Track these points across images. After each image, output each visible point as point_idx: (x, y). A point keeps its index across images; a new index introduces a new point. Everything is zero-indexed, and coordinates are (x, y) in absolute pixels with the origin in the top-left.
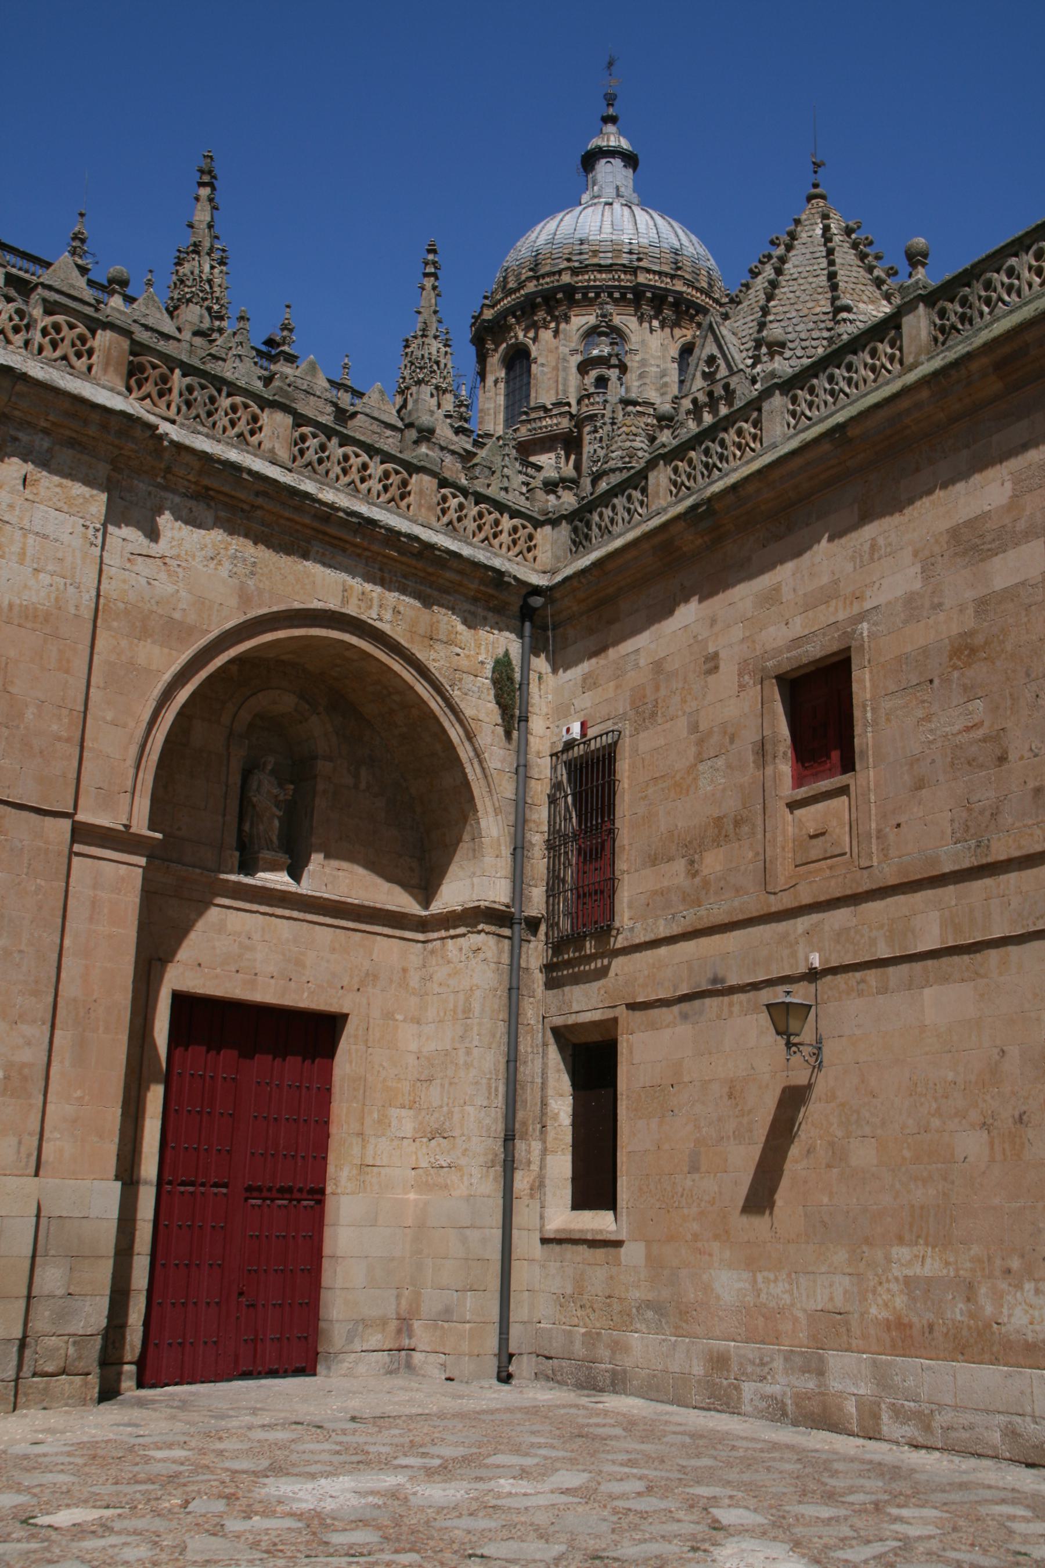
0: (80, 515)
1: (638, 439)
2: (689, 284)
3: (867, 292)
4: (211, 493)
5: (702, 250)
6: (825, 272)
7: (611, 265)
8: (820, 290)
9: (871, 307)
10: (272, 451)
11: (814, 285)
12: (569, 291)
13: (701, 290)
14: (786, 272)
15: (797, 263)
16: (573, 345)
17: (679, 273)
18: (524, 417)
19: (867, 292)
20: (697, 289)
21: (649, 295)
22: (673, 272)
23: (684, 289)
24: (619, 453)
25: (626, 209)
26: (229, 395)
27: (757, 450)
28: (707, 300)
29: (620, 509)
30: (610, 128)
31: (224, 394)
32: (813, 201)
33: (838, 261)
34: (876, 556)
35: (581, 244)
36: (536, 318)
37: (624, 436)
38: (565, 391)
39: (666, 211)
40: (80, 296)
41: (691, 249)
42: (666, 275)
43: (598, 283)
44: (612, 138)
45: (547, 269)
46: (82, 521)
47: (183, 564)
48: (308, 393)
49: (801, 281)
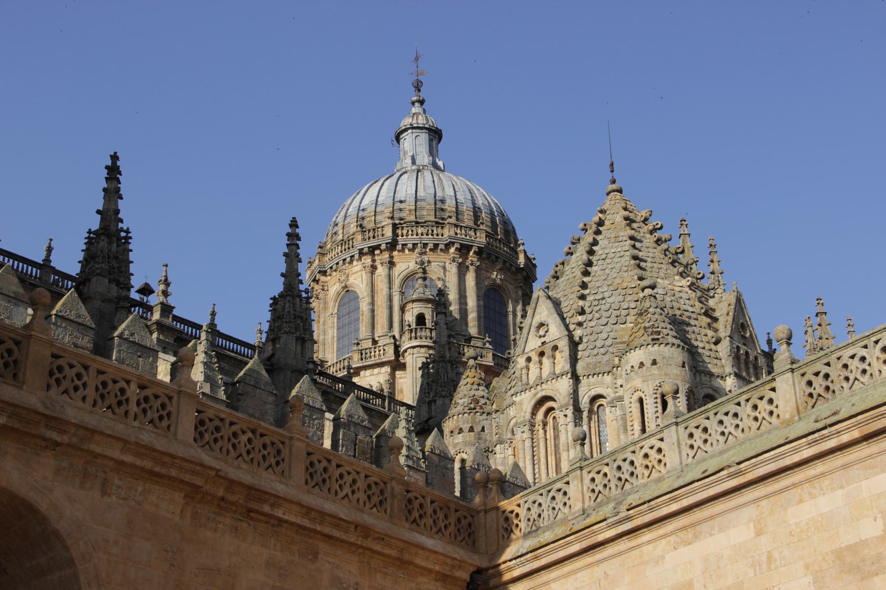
1: (481, 388)
4: (252, 514)
6: (628, 253)
7: (425, 222)
15: (604, 246)
21: (457, 246)
24: (466, 400)
29: (544, 506)
32: (612, 194)
34: (773, 566)
44: (420, 117)
48: (255, 387)
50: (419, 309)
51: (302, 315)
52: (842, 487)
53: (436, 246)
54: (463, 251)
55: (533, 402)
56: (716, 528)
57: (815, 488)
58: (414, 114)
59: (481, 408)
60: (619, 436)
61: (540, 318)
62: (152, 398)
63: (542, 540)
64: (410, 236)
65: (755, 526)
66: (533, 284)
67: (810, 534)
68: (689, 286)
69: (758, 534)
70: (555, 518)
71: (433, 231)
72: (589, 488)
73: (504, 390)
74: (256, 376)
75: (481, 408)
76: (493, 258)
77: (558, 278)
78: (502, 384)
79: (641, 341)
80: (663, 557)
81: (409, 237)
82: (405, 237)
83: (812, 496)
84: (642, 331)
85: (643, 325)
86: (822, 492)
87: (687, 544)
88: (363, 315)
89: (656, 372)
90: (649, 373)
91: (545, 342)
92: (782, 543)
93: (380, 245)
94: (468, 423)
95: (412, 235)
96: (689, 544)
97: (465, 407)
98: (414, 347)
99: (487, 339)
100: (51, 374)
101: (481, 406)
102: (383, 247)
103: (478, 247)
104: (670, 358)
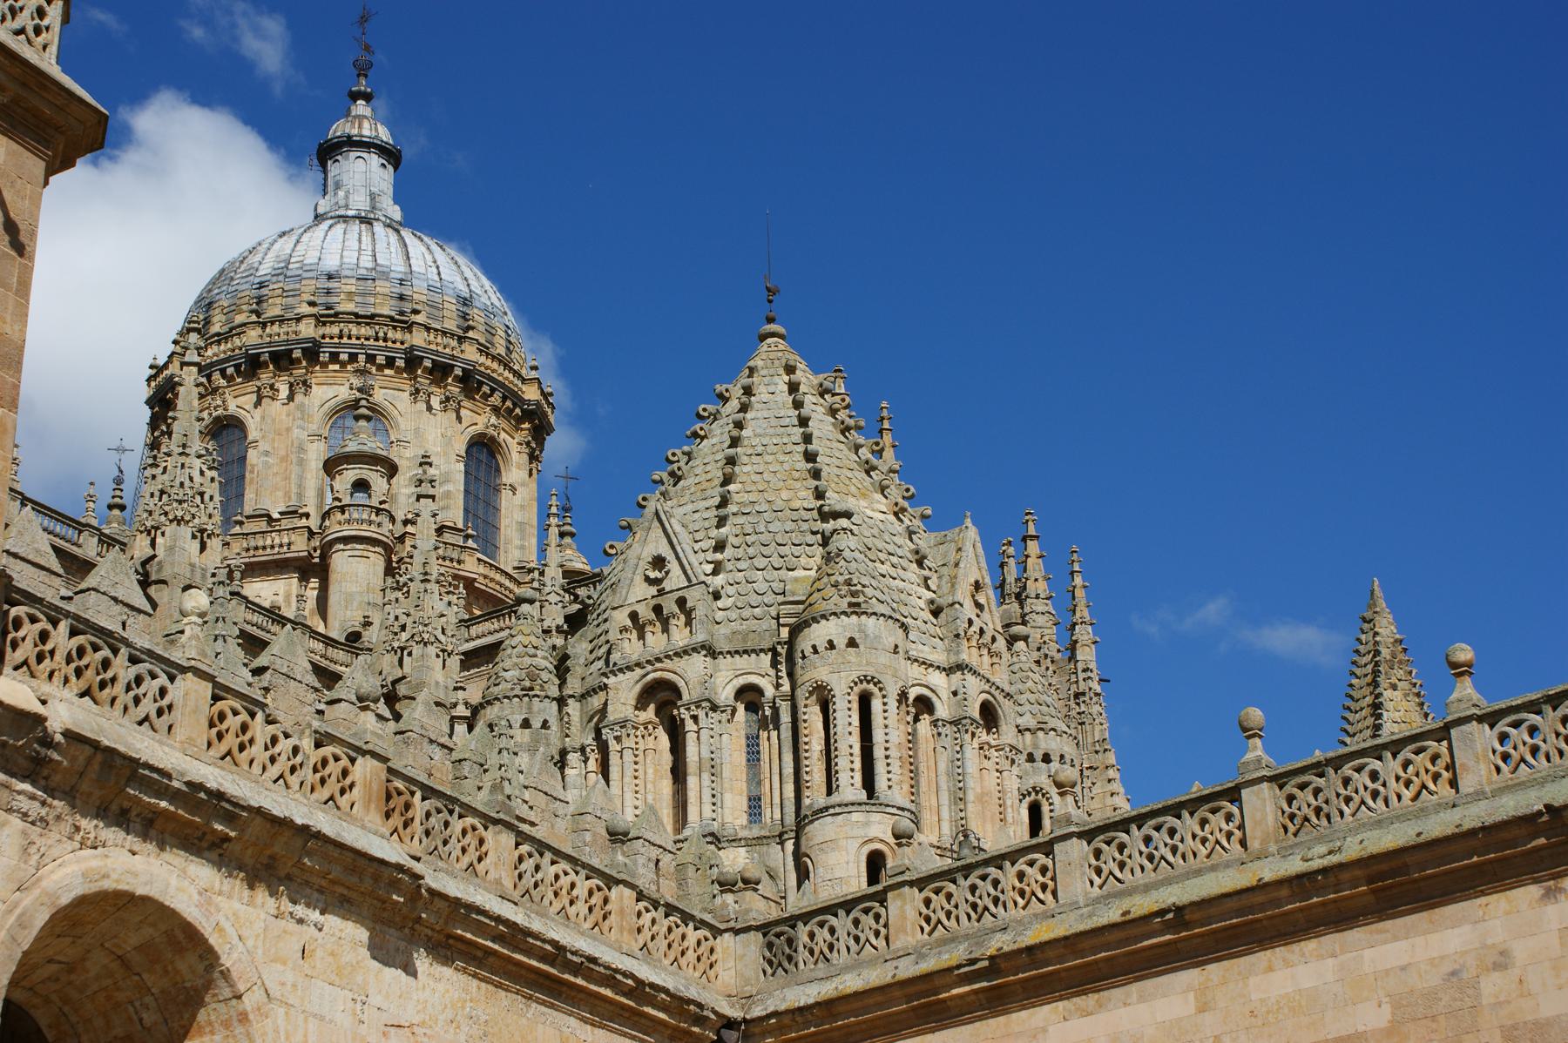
0: (349, 987)
2: (484, 350)
3: (854, 480)
6: (801, 448)
7: (373, 316)
8: (797, 475)
9: (863, 503)
10: (498, 882)
11: (786, 466)
13: (495, 358)
14: (746, 443)
15: (759, 431)
16: (313, 428)
18: (237, 529)
19: (854, 480)
20: (494, 358)
21: (428, 363)
22: (460, 333)
25: (390, 231)
26: (461, 817)
27: (1047, 902)
28: (506, 373)
30: (361, 107)
31: (456, 815)
32: (770, 340)
33: (816, 433)
37: (520, 649)
38: (300, 495)
40: (47, 566)
41: (484, 299)
43: (354, 341)
44: (366, 124)
45: (277, 311)
46: (350, 995)
47: (428, 1032)
48: (288, 677)
49: (769, 458)
50: (358, 471)
51: (204, 489)
52: (1334, 956)
53: (390, 362)
54: (435, 373)
55: (638, 688)
56: (1135, 995)
57: (1293, 952)
58: (355, 117)
59: (542, 689)
61: (657, 548)
62: (331, 760)
63: (840, 987)
64: (345, 339)
65: (1196, 998)
66: (547, 437)
67: (1281, 1017)
68: (896, 514)
69: (1202, 1009)
70: (858, 954)
71: (386, 334)
72: (920, 914)
73: (582, 661)
74: (289, 658)
75: (542, 689)
77: (679, 479)
78: (579, 651)
79: (829, 606)
80: (1044, 1030)
81: (342, 341)
82: (336, 340)
83: (1288, 964)
84: (830, 591)
86: (1303, 960)
87: (1084, 1014)
88: (252, 472)
89: (853, 660)
90: (840, 660)
91: (664, 589)
92: (1238, 1026)
93: (291, 351)
94: (521, 714)
96: (1092, 1014)
97: (514, 684)
98: (346, 540)
99: (470, 531)
100: (212, 725)
101: (541, 686)
102: (297, 354)
103: (463, 369)
104: (876, 637)
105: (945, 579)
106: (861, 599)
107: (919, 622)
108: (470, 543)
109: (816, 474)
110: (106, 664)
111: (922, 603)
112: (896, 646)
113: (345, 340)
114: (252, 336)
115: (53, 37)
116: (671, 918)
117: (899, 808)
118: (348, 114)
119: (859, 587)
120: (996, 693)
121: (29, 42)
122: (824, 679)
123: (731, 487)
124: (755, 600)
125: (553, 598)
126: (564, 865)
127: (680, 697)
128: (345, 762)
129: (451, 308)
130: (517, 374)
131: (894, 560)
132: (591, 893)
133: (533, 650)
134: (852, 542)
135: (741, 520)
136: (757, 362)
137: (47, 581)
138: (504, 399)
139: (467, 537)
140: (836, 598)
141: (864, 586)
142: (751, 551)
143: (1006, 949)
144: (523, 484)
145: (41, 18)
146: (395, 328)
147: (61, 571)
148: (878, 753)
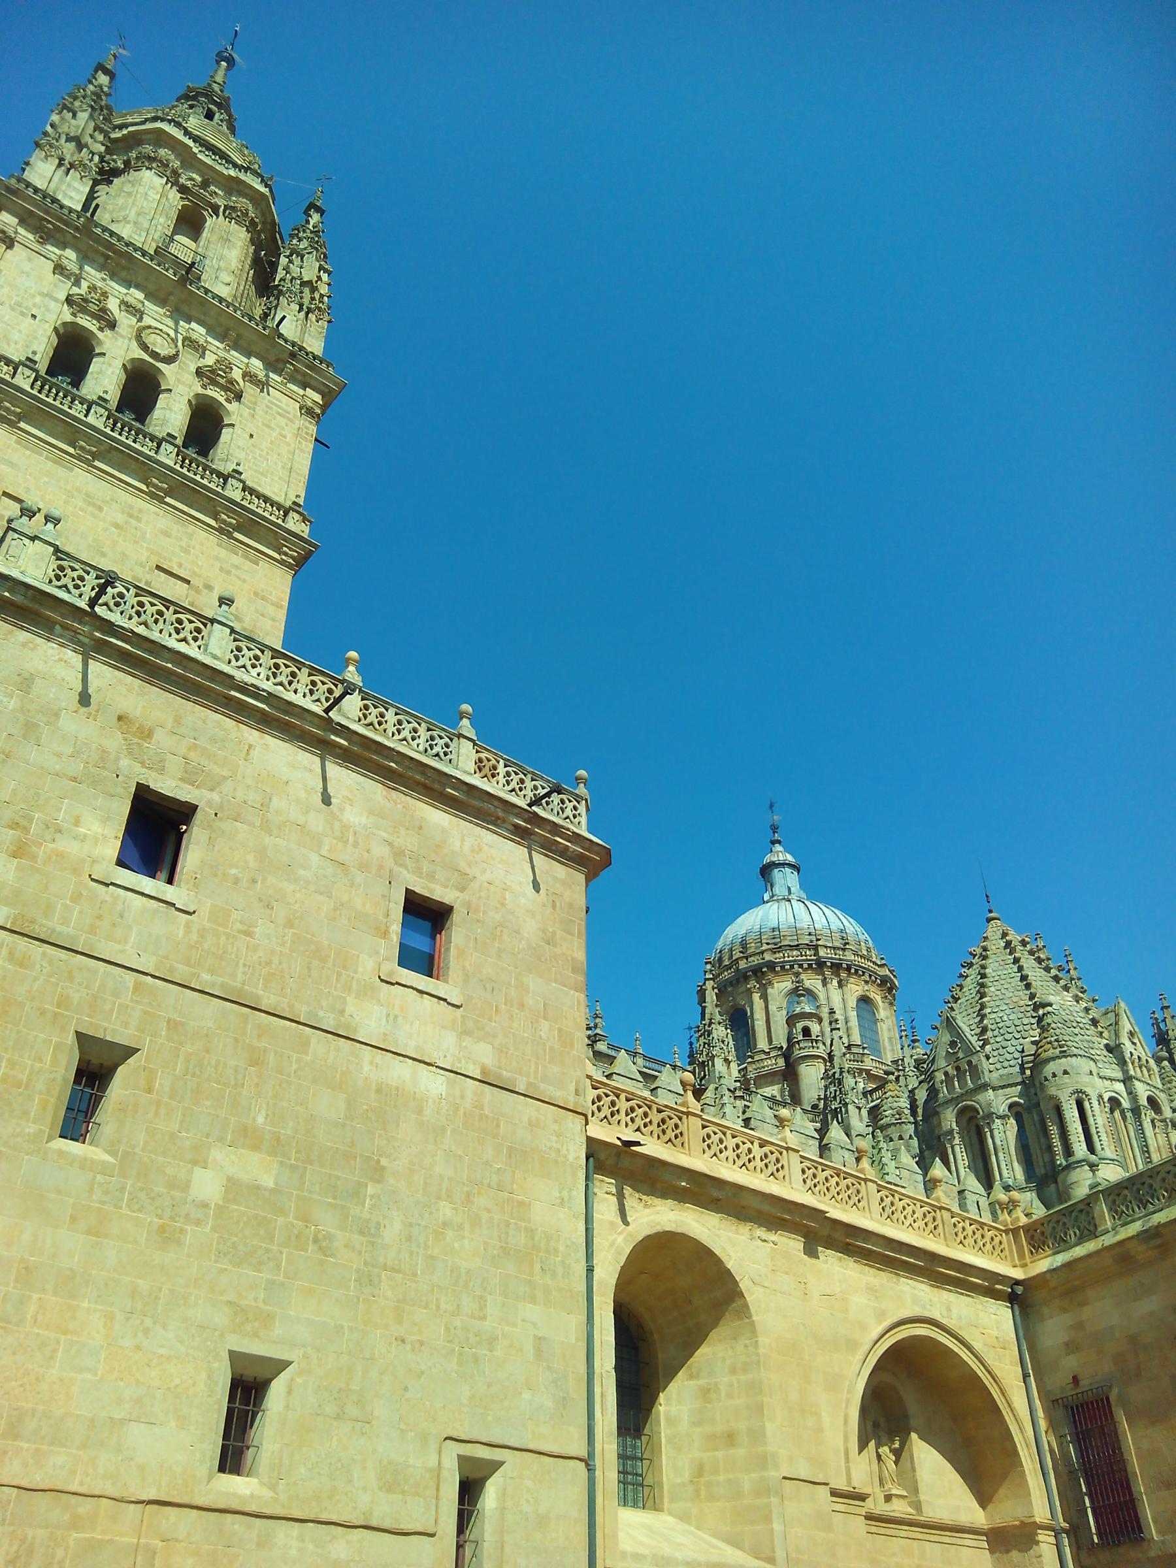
2: (856, 954)
4: (850, 1247)
5: (859, 929)
7: (798, 945)
9: (1058, 998)
12: (771, 966)
15: (994, 969)
17: (847, 946)
18: (750, 1060)
21: (829, 964)
22: (842, 946)
23: (852, 957)
28: (869, 963)
30: (778, 848)
32: (992, 922)
35: (773, 931)
36: (748, 986)
37: (890, 1099)
39: (829, 903)
42: (839, 948)
43: (791, 959)
44: (780, 854)
49: (1003, 982)
53: (810, 966)
60: (1038, 1139)
76: (860, 973)
85: (1049, 1039)
95: (788, 957)
99: (865, 1046)
100: (704, 1141)
105: (1113, 1032)
106: (1065, 1049)
107: (1102, 1057)
108: (866, 1051)
109: (1028, 986)
110: (646, 1115)
111: (1102, 1046)
112: (1091, 1071)
113: (786, 959)
114: (743, 964)
115: (583, 820)
116: (973, 1226)
117: (1110, 1160)
118: (771, 851)
119: (1064, 1042)
120: (1154, 1090)
121: (544, 809)
122: (1055, 1093)
123: (985, 1000)
124: (1009, 1057)
125: (911, 1074)
126: (907, 1201)
127: (979, 1113)
128: (776, 1154)
129: (837, 936)
130: (874, 963)
131: (1081, 1025)
132: (925, 1215)
133: (897, 1099)
134: (1055, 1018)
135: (994, 1016)
136: (989, 934)
137: (635, 1085)
138: (870, 976)
139: (864, 1048)
140: (1052, 1051)
141: (1066, 1041)
142: (1001, 1031)
143: (1162, 1222)
144: (887, 1018)
145: (563, 804)
146: (810, 950)
147: (642, 1080)
148: (1093, 1131)
